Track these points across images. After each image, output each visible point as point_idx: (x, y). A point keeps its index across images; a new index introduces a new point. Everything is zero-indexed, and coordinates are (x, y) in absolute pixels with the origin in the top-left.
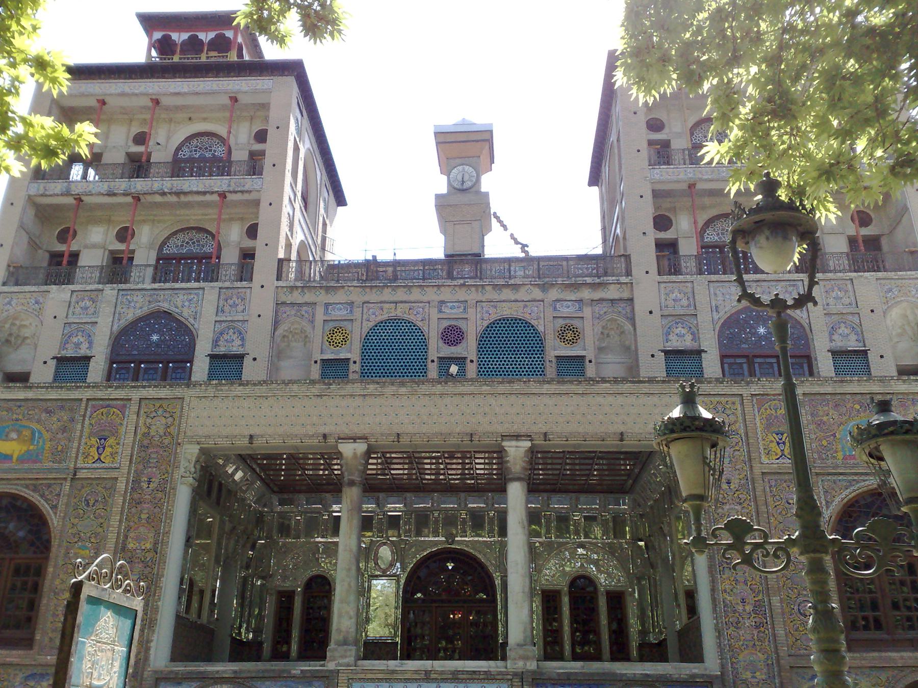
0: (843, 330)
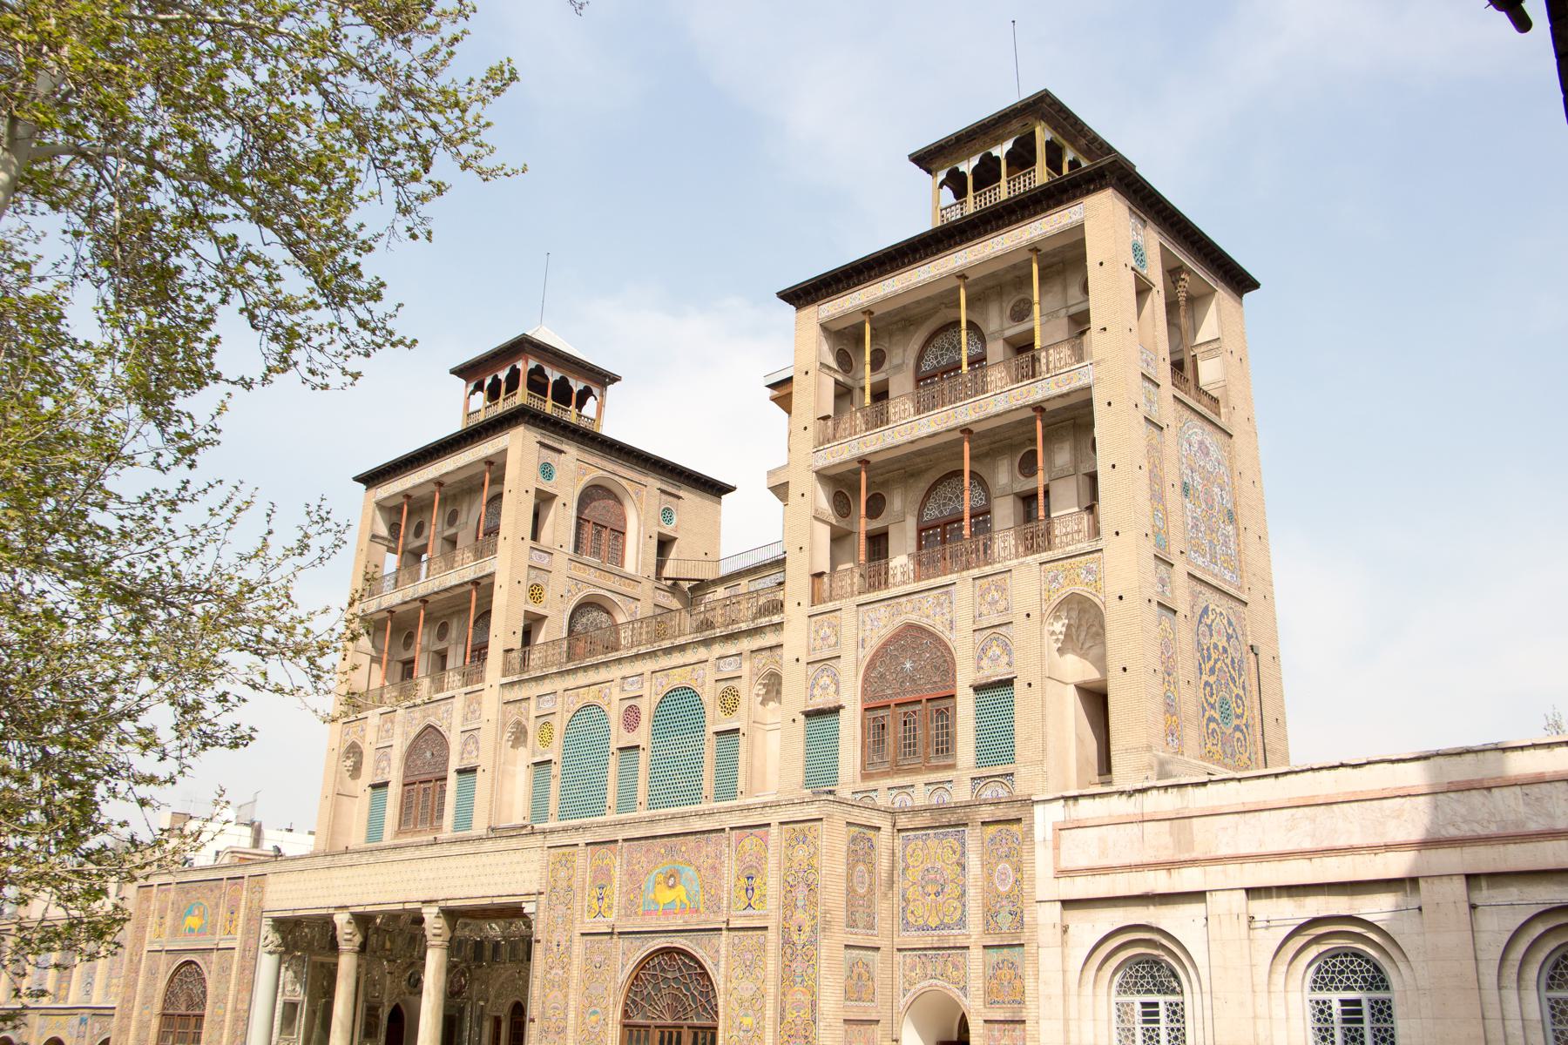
0: (996, 650)
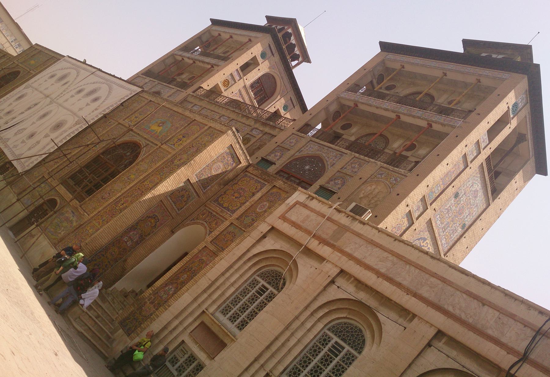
0: (339, 182)
